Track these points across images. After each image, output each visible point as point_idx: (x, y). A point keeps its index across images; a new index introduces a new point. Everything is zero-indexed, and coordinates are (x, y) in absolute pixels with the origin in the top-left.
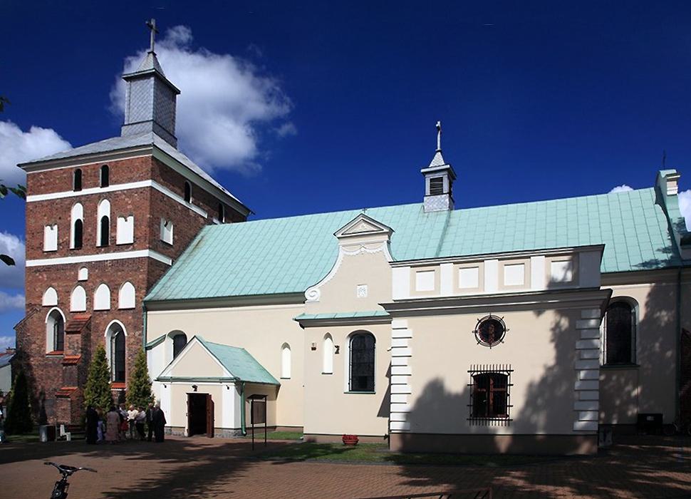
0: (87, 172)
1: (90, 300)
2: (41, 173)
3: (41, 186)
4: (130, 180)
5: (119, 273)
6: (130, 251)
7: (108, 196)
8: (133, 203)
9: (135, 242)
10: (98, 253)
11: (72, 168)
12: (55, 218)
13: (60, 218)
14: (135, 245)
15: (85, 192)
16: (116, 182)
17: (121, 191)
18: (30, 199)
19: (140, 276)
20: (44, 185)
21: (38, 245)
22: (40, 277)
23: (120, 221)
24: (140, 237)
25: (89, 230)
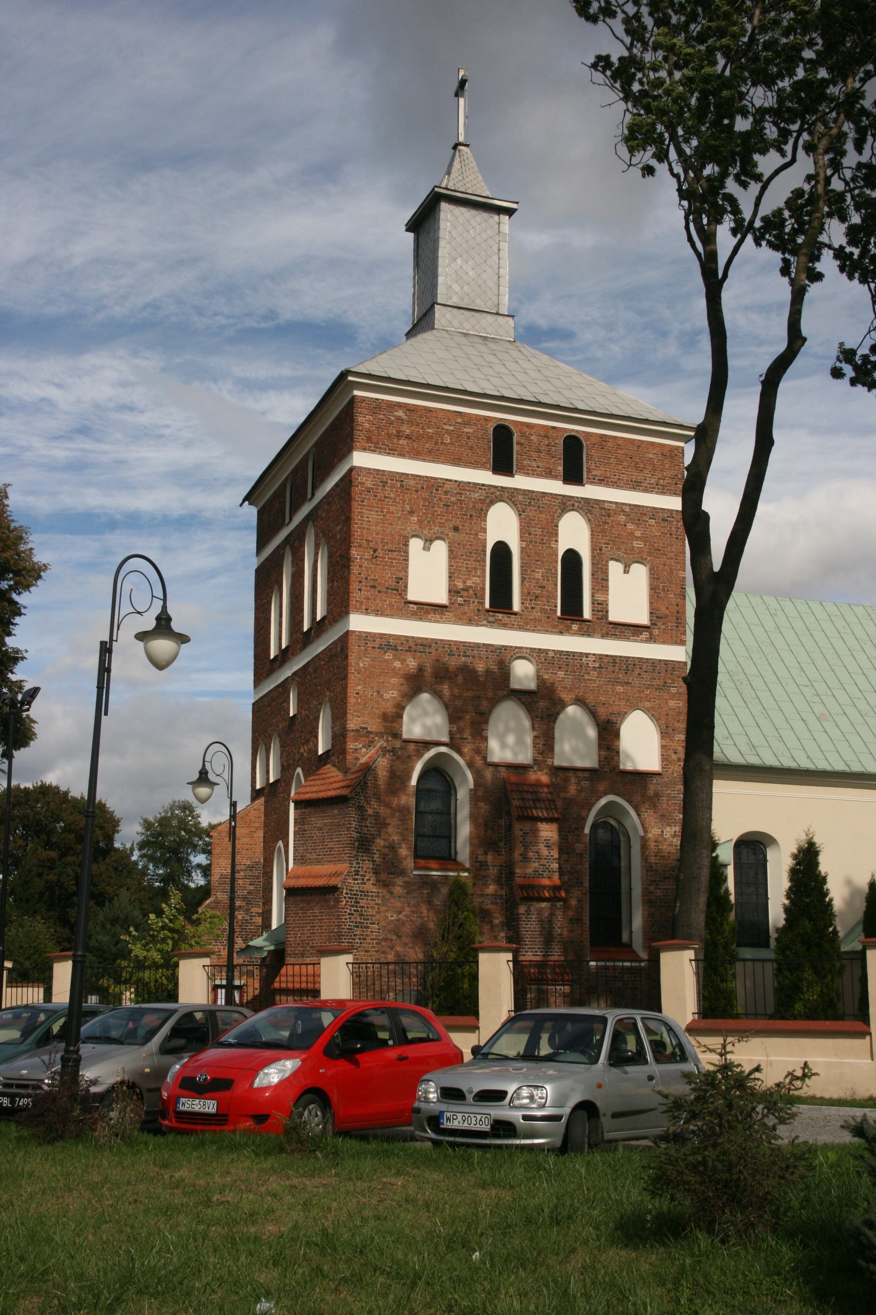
0: (530, 441)
1: (545, 742)
2: (400, 405)
3: (399, 437)
4: (636, 486)
5: (620, 689)
6: (642, 641)
7: (587, 507)
8: (644, 539)
9: (654, 624)
10: (561, 633)
11: (486, 419)
12: (441, 525)
13: (456, 529)
14: (656, 632)
15: (520, 482)
16: (602, 481)
17: (617, 503)
18: (361, 459)
19: (672, 703)
20: (408, 437)
21: (392, 583)
22: (397, 664)
23: (615, 568)
24: (666, 616)
25: (539, 576)
